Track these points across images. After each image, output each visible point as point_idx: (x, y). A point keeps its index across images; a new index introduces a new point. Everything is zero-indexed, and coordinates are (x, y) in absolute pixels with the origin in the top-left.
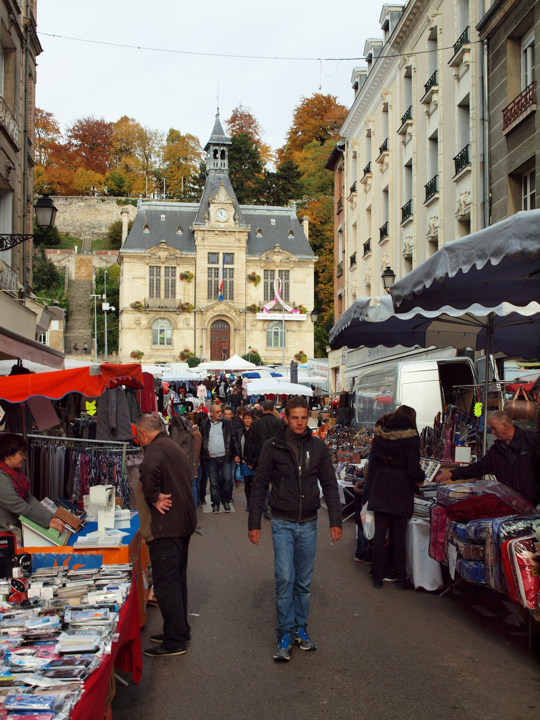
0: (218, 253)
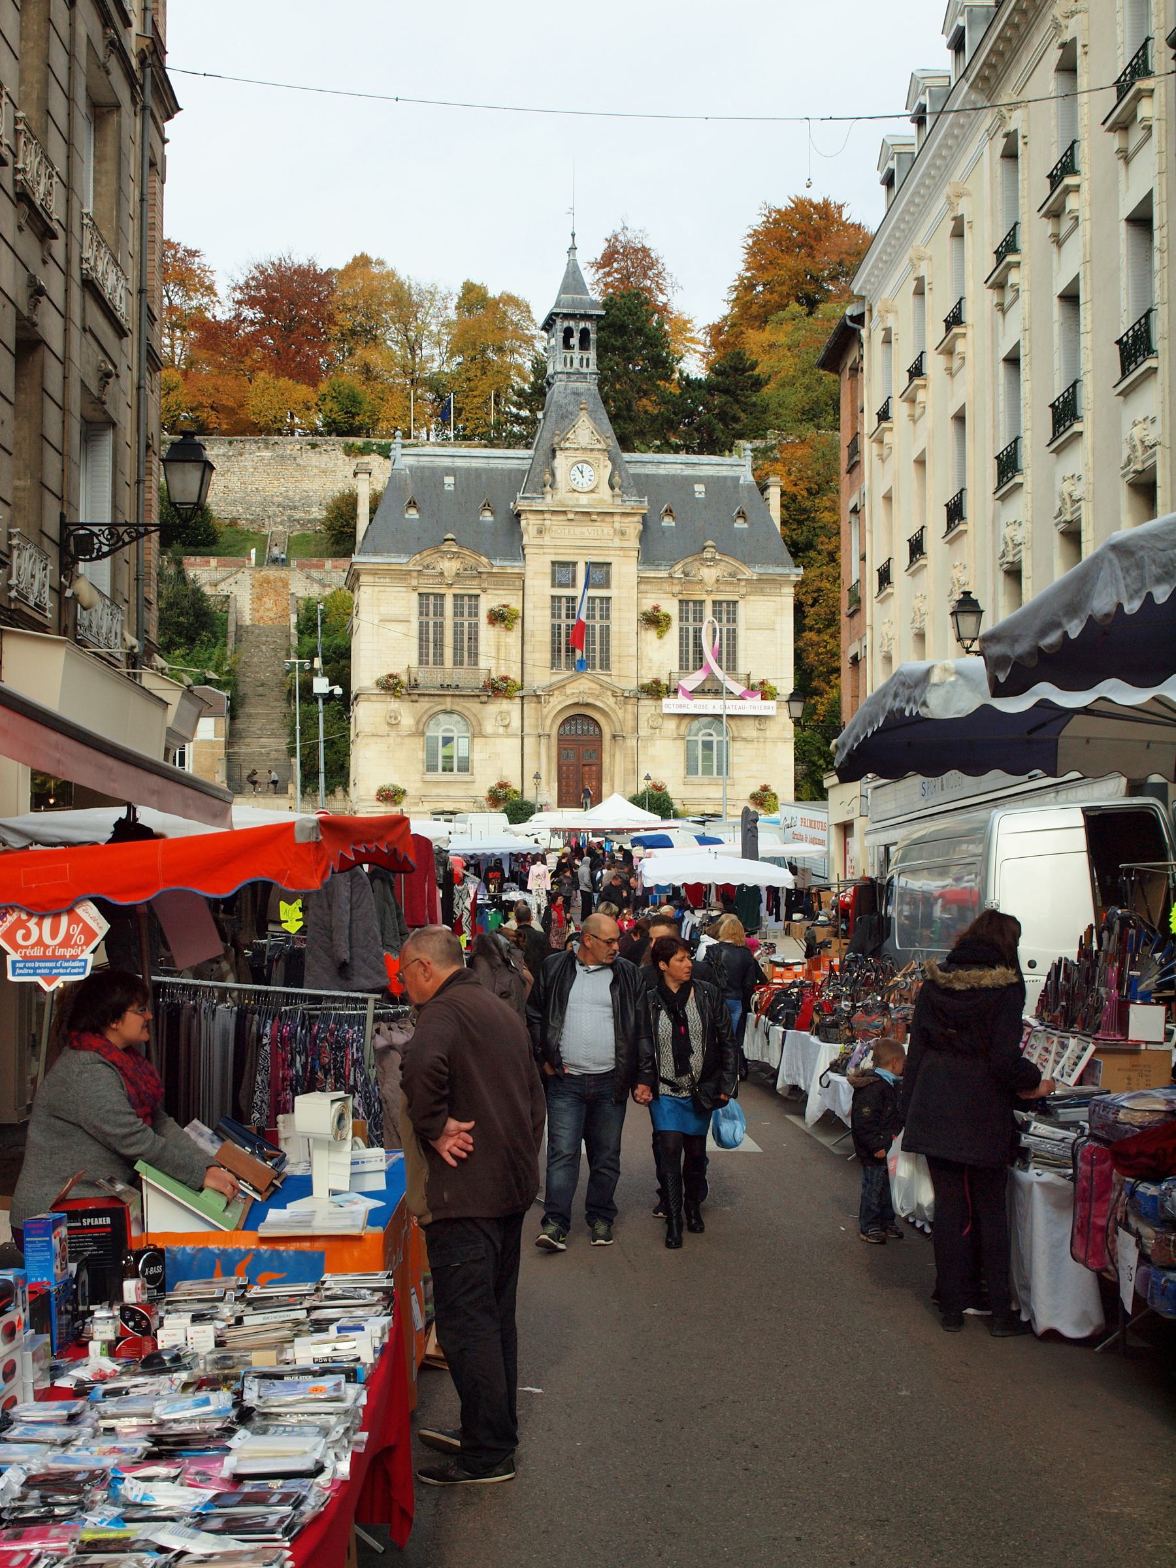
0: (575, 564)
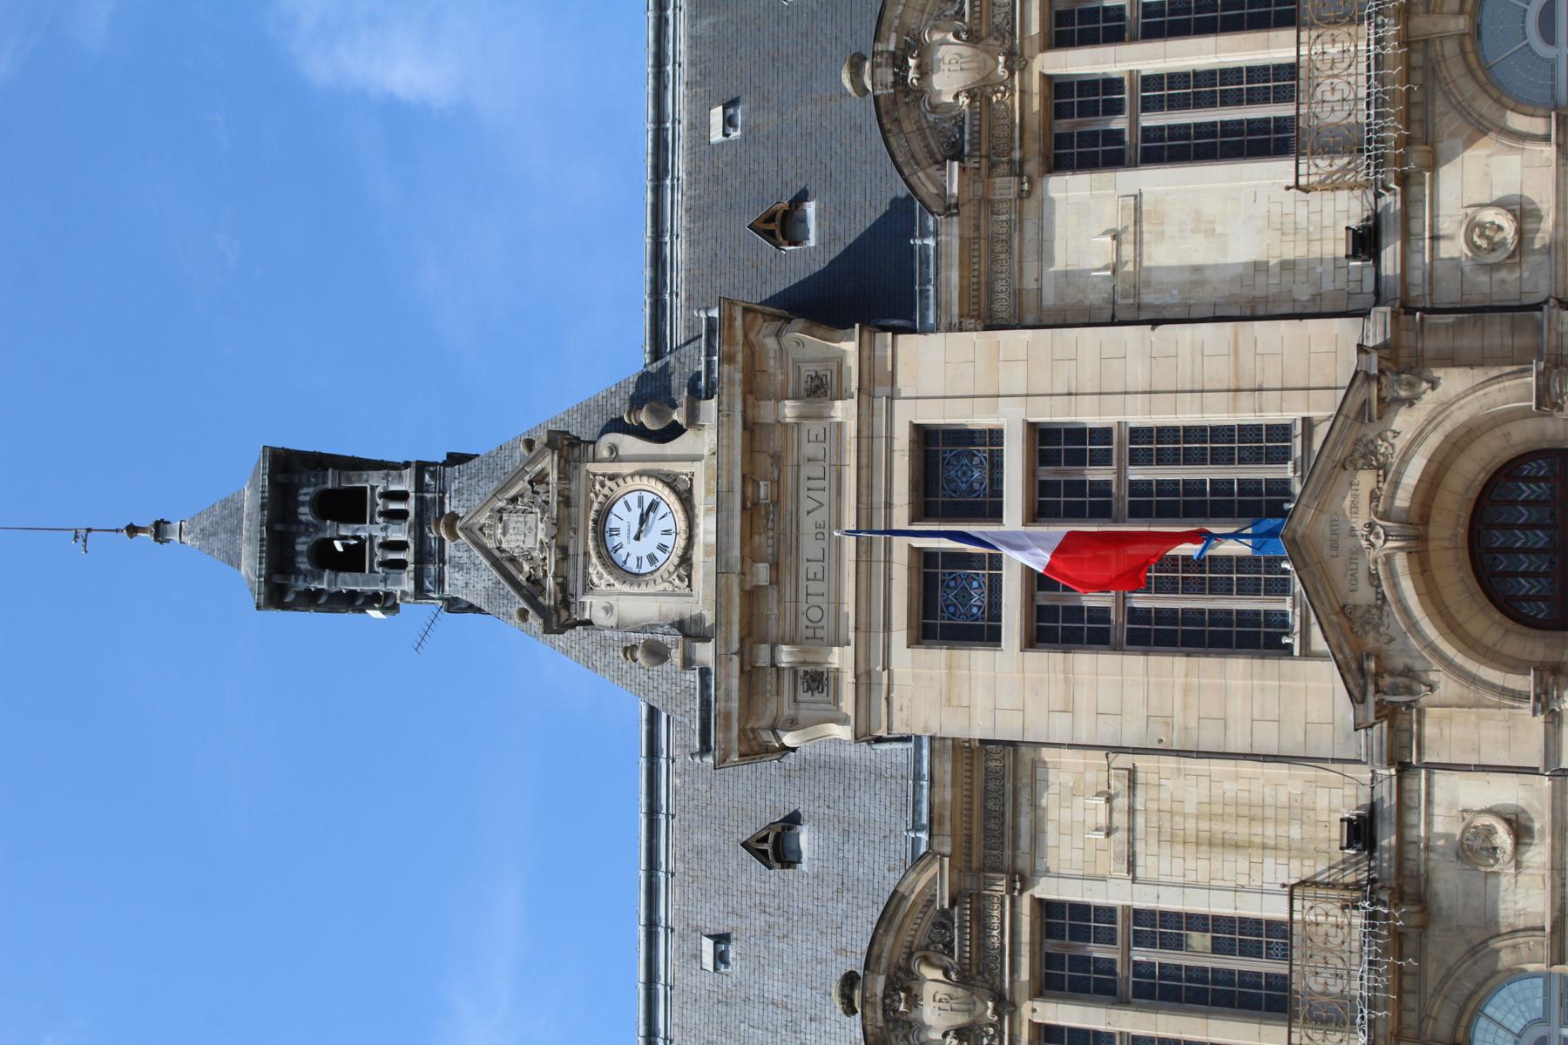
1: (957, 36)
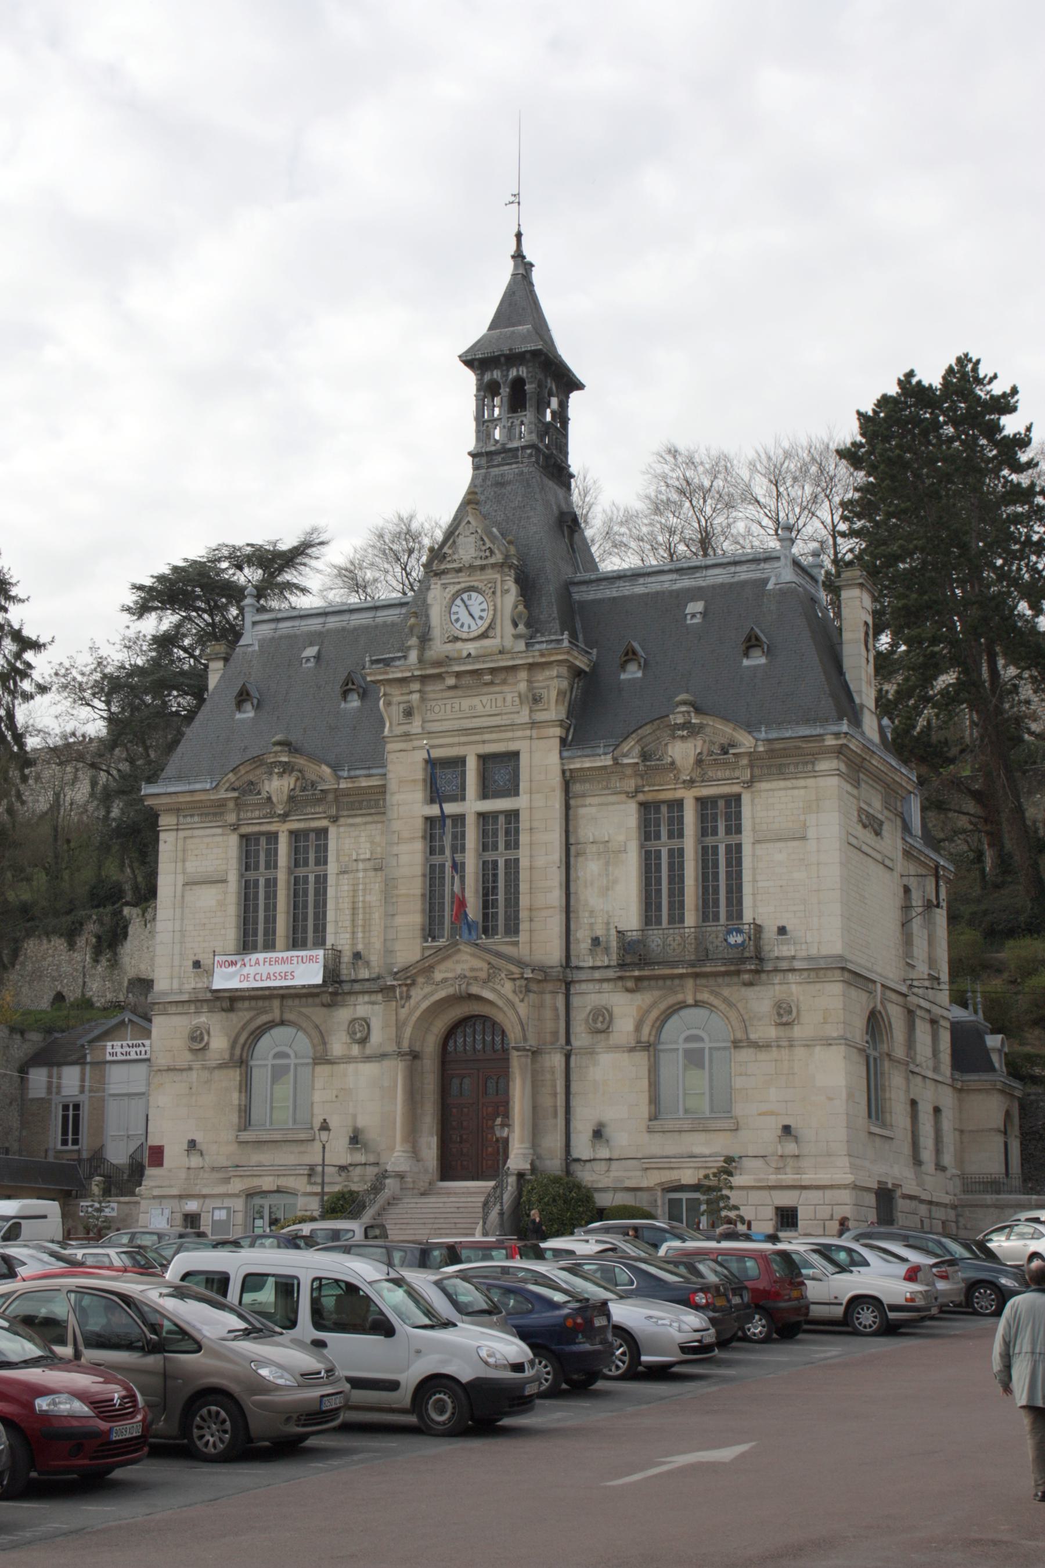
0: (461, 761)
1: (699, 754)
